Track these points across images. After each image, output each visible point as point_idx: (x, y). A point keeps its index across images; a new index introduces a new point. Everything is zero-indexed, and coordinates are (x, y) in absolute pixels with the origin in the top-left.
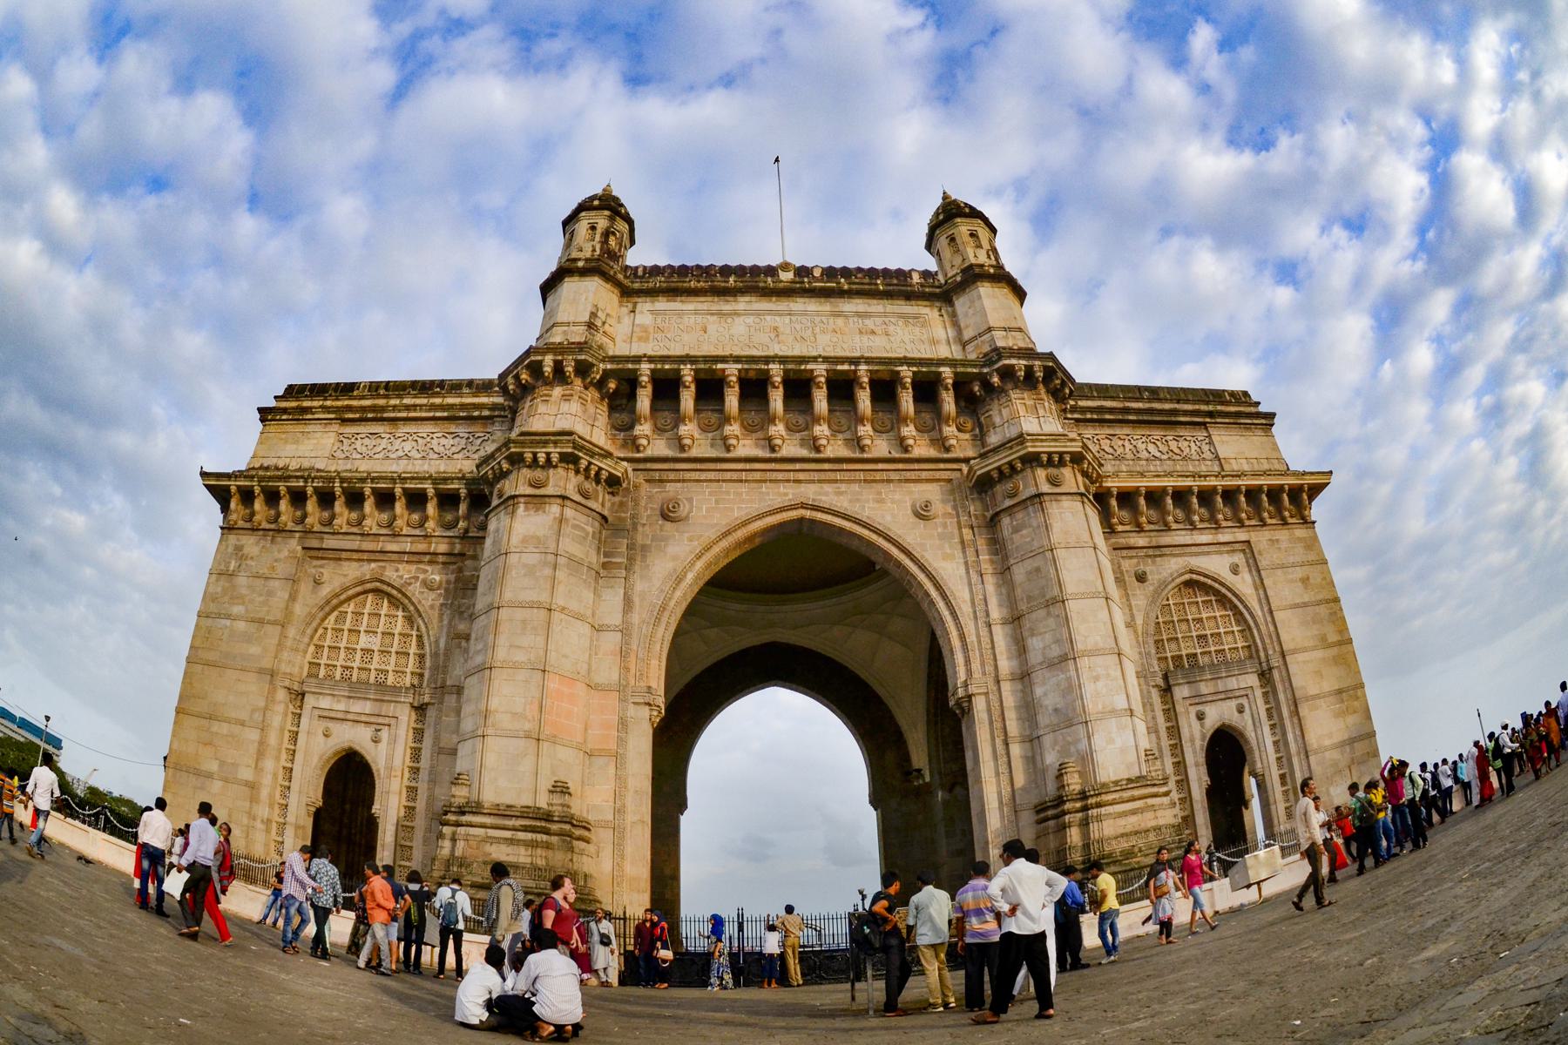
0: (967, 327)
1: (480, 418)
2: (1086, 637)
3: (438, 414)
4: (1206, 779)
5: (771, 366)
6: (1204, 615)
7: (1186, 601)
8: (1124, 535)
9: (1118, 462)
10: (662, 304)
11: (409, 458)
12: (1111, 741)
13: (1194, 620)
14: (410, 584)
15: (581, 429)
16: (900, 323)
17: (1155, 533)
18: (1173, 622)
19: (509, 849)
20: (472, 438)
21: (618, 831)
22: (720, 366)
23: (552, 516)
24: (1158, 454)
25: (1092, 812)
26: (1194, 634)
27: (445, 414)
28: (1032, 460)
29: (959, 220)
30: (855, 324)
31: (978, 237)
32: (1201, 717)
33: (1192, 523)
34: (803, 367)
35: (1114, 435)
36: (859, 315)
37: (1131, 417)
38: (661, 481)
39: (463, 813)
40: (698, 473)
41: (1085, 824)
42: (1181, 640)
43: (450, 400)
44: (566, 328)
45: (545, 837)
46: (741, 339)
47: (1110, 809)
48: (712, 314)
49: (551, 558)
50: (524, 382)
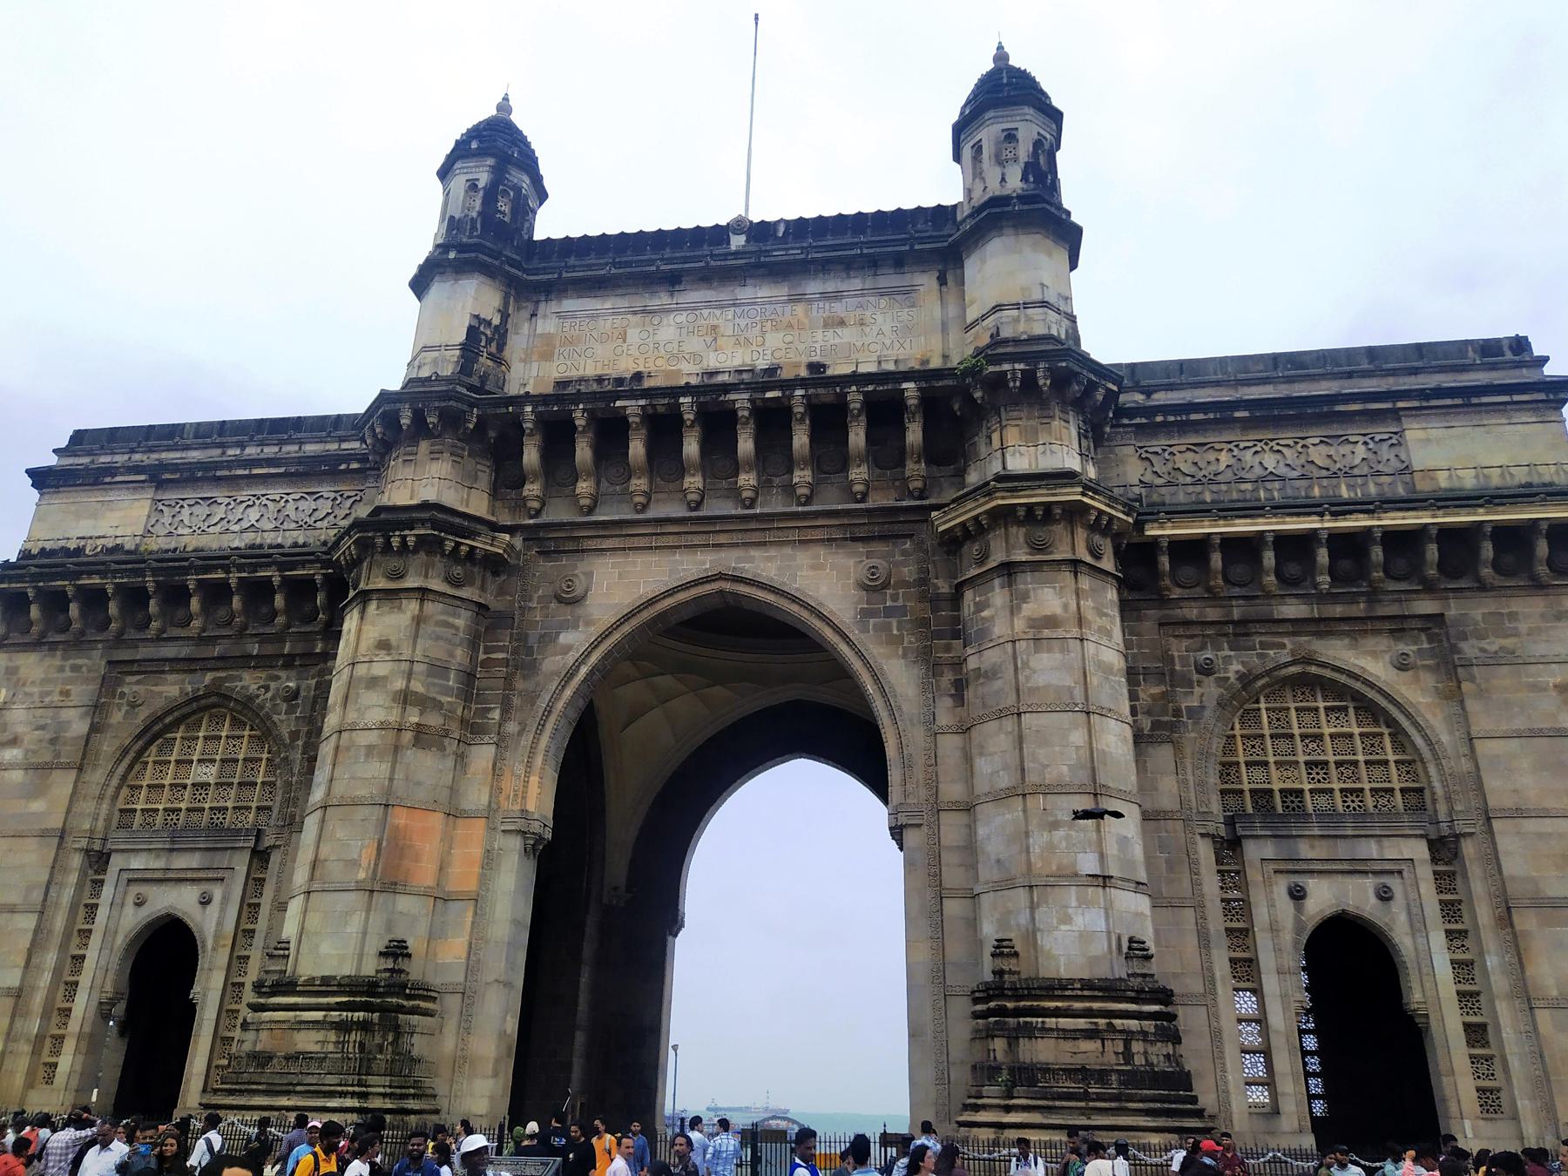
0: (972, 303)
1: (348, 471)
2: (1048, 766)
5: (682, 400)
6: (1327, 731)
7: (1292, 705)
8: (1185, 604)
9: (1199, 488)
10: (570, 304)
12: (1067, 919)
13: (1303, 737)
14: (258, 696)
15: (451, 498)
17: (1241, 602)
18: (1263, 736)
19: (320, 1036)
20: (339, 499)
21: (467, 994)
22: (618, 403)
23: (409, 615)
24: (1282, 470)
26: (1302, 758)
28: (1003, 516)
29: (991, 114)
30: (821, 310)
31: (1018, 141)
32: (1298, 895)
33: (1315, 586)
34: (721, 399)
35: (1206, 444)
36: (826, 296)
37: (1237, 414)
38: (554, 552)
39: (273, 994)
40: (599, 540)
41: (1013, 1038)
42: (1273, 767)
44: (436, 354)
47: (1051, 1022)
48: (635, 313)
49: (405, 666)
50: (379, 436)
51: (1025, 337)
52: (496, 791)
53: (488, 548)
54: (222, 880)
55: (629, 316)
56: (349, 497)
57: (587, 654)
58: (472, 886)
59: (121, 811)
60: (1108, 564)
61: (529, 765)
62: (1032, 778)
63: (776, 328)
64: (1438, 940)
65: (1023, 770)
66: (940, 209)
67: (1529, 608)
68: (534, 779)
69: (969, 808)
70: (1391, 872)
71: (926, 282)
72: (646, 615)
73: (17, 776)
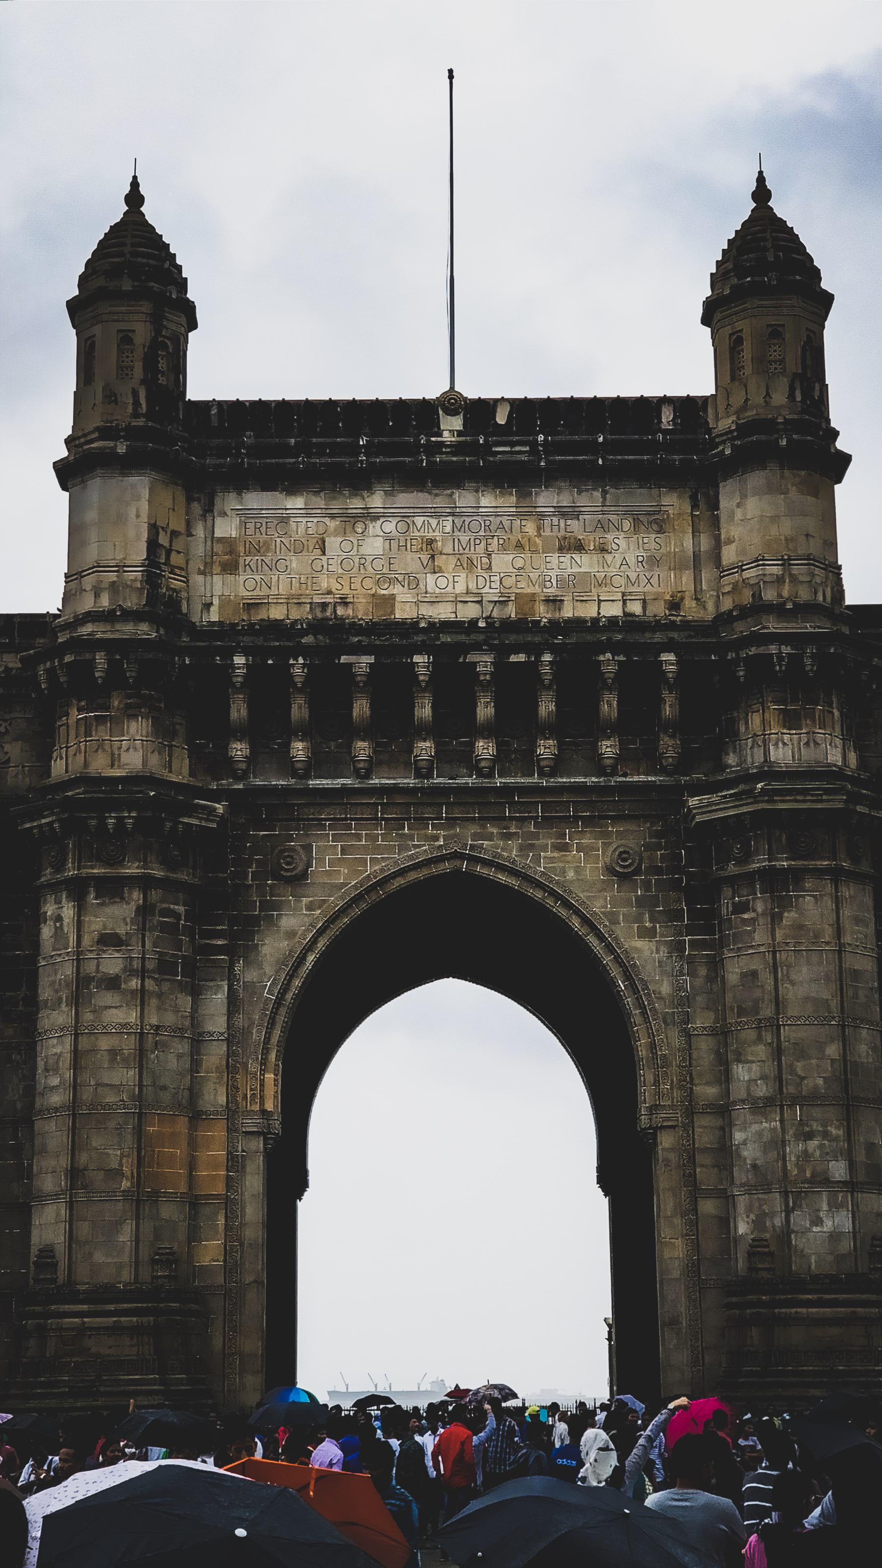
0: (730, 541)
2: (803, 1078)
5: (417, 659)
12: (818, 1222)
16: (627, 525)
22: (344, 659)
23: (133, 906)
30: (554, 528)
46: (378, 565)
48: (332, 517)
49: (136, 964)
51: (789, 606)
52: (232, 1090)
55: (327, 520)
57: (314, 941)
61: (264, 1063)
63: (503, 548)
66: (689, 401)
68: (270, 1076)
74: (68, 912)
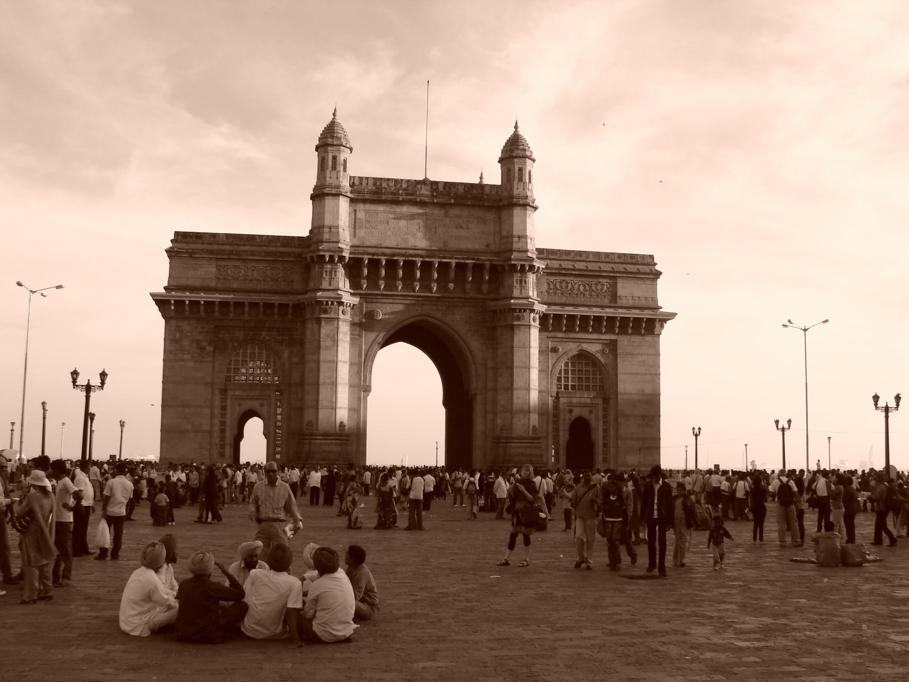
3: (269, 259)
4: (567, 436)
6: (584, 369)
10: (369, 207)
11: (258, 280)
12: (520, 421)
16: (475, 222)
25: (508, 444)
27: (272, 259)
29: (516, 160)
36: (457, 216)
38: (371, 302)
43: (271, 249)
45: (339, 441)
48: (391, 214)
51: (521, 250)
53: (354, 303)
54: (266, 399)
55: (390, 215)
56: (289, 270)
58: (356, 406)
59: (226, 376)
60: (537, 323)
62: (515, 386)
64: (601, 423)
65: (512, 384)
67: (637, 339)
69: (495, 390)
70: (593, 407)
71: (490, 216)
72: (400, 326)
73: (191, 364)
74: (316, 326)
